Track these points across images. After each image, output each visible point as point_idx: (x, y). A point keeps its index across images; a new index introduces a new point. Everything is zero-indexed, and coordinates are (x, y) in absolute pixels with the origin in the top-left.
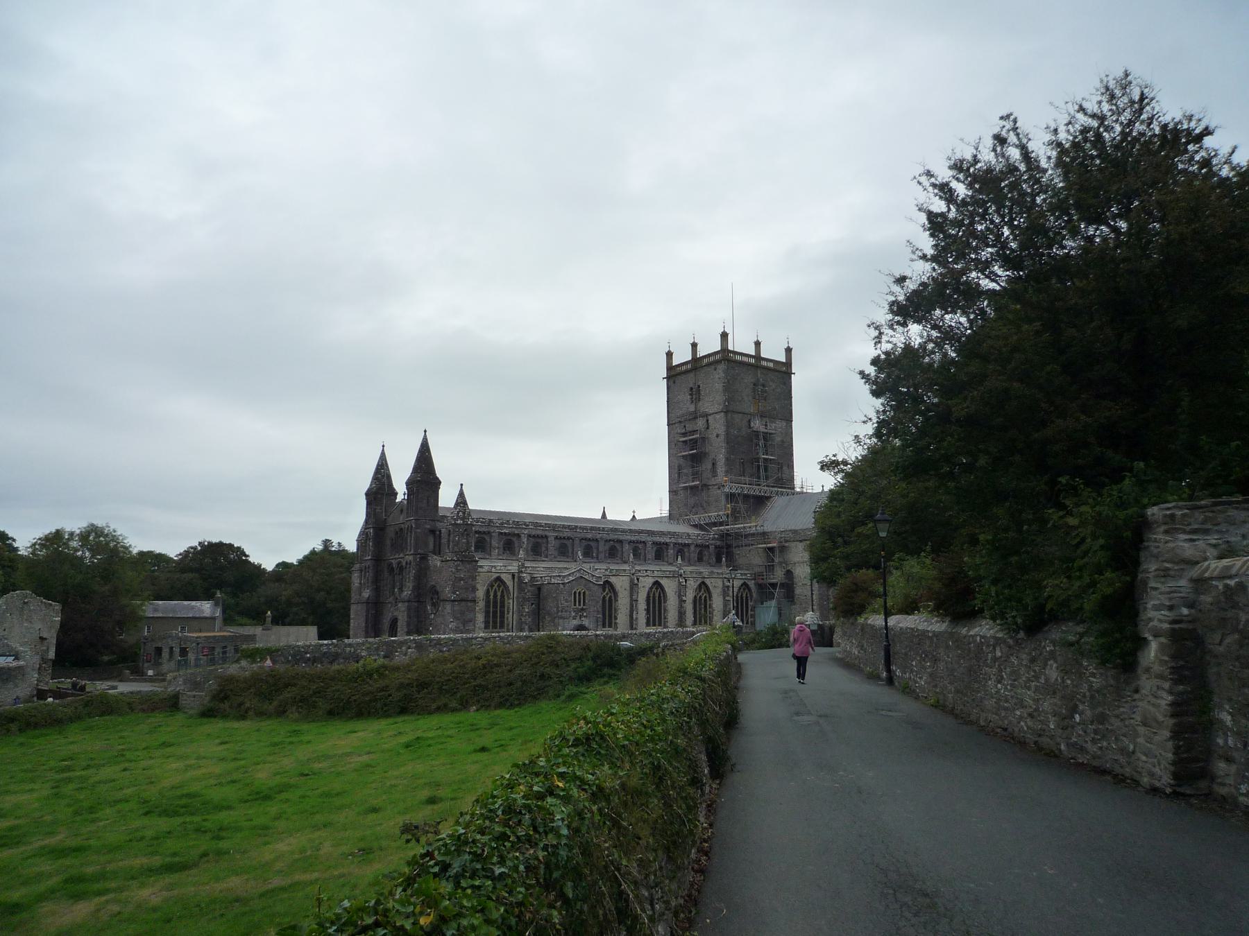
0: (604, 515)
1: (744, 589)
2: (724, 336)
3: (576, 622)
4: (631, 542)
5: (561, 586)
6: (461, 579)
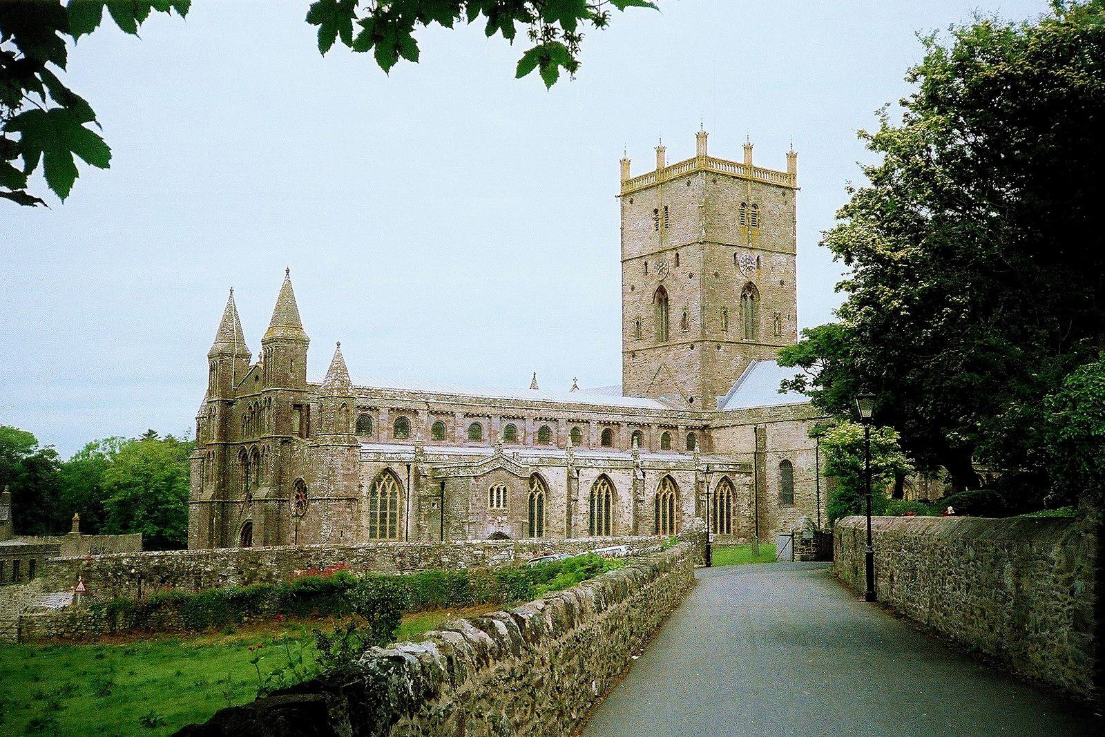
0: (534, 386)
1: (725, 486)
2: (702, 137)
3: (492, 530)
4: (569, 421)
5: (473, 480)
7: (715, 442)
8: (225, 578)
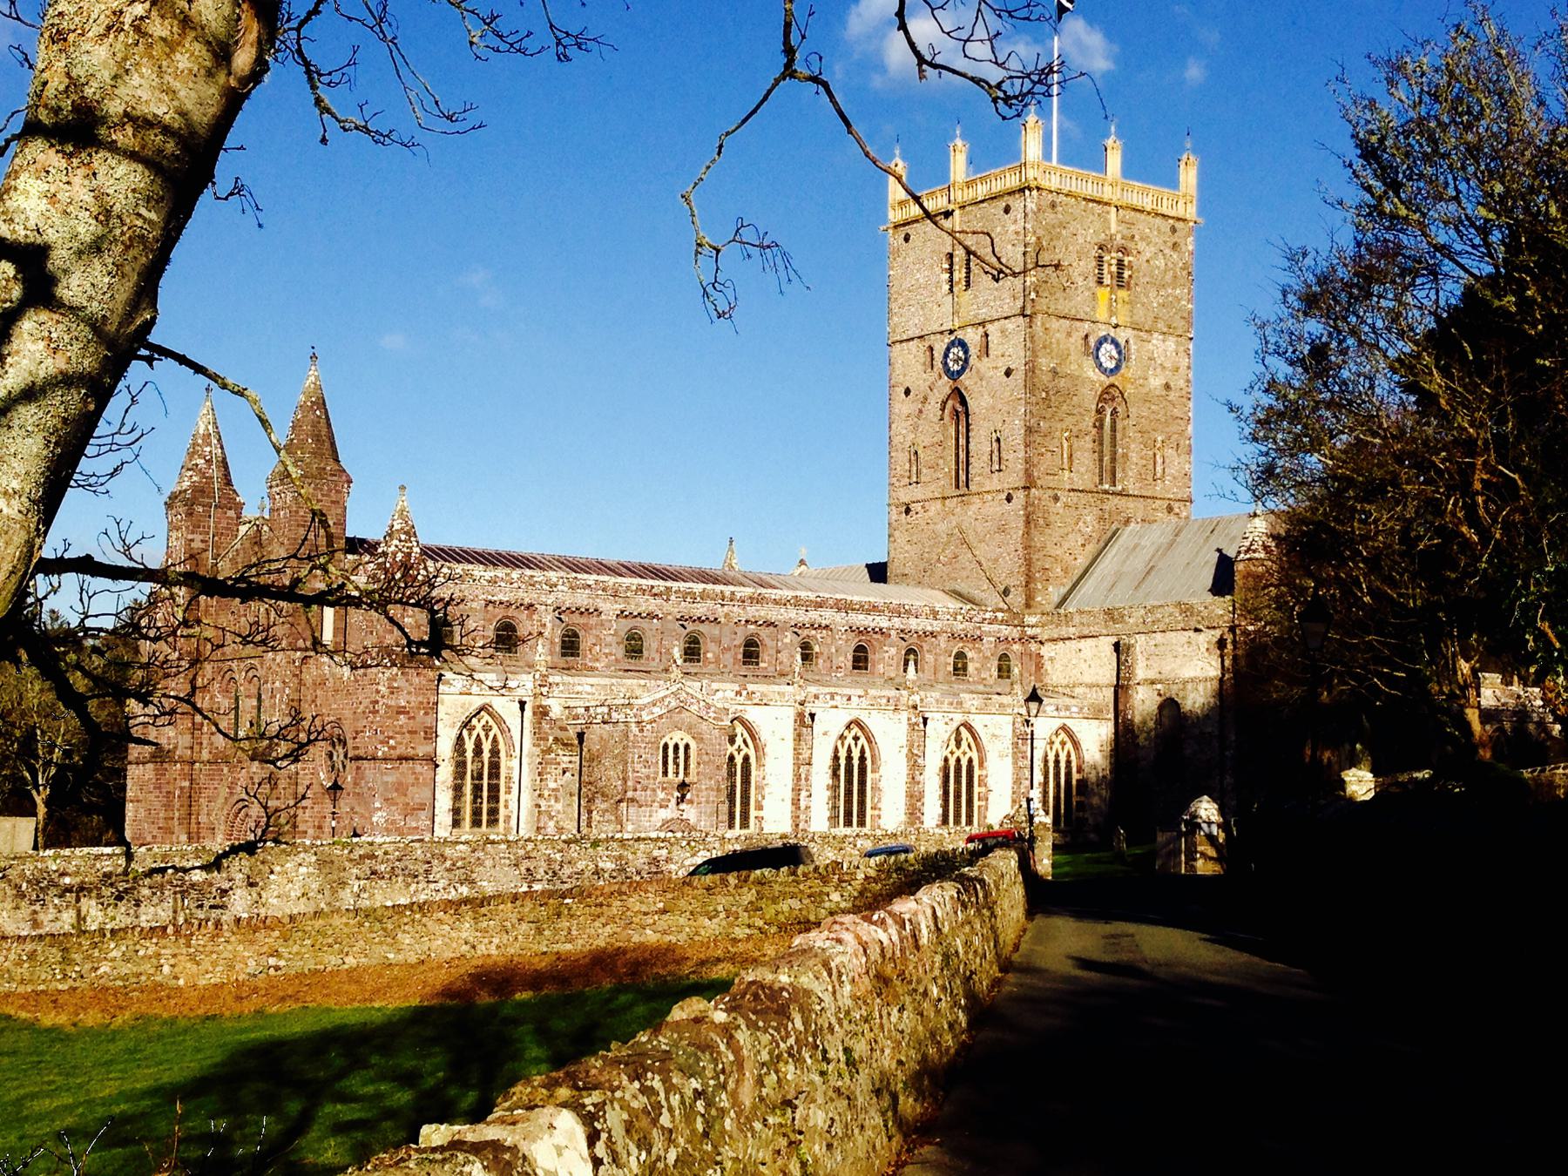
3: (665, 814)
6: (401, 711)
7: (1048, 666)
8: (224, 892)
